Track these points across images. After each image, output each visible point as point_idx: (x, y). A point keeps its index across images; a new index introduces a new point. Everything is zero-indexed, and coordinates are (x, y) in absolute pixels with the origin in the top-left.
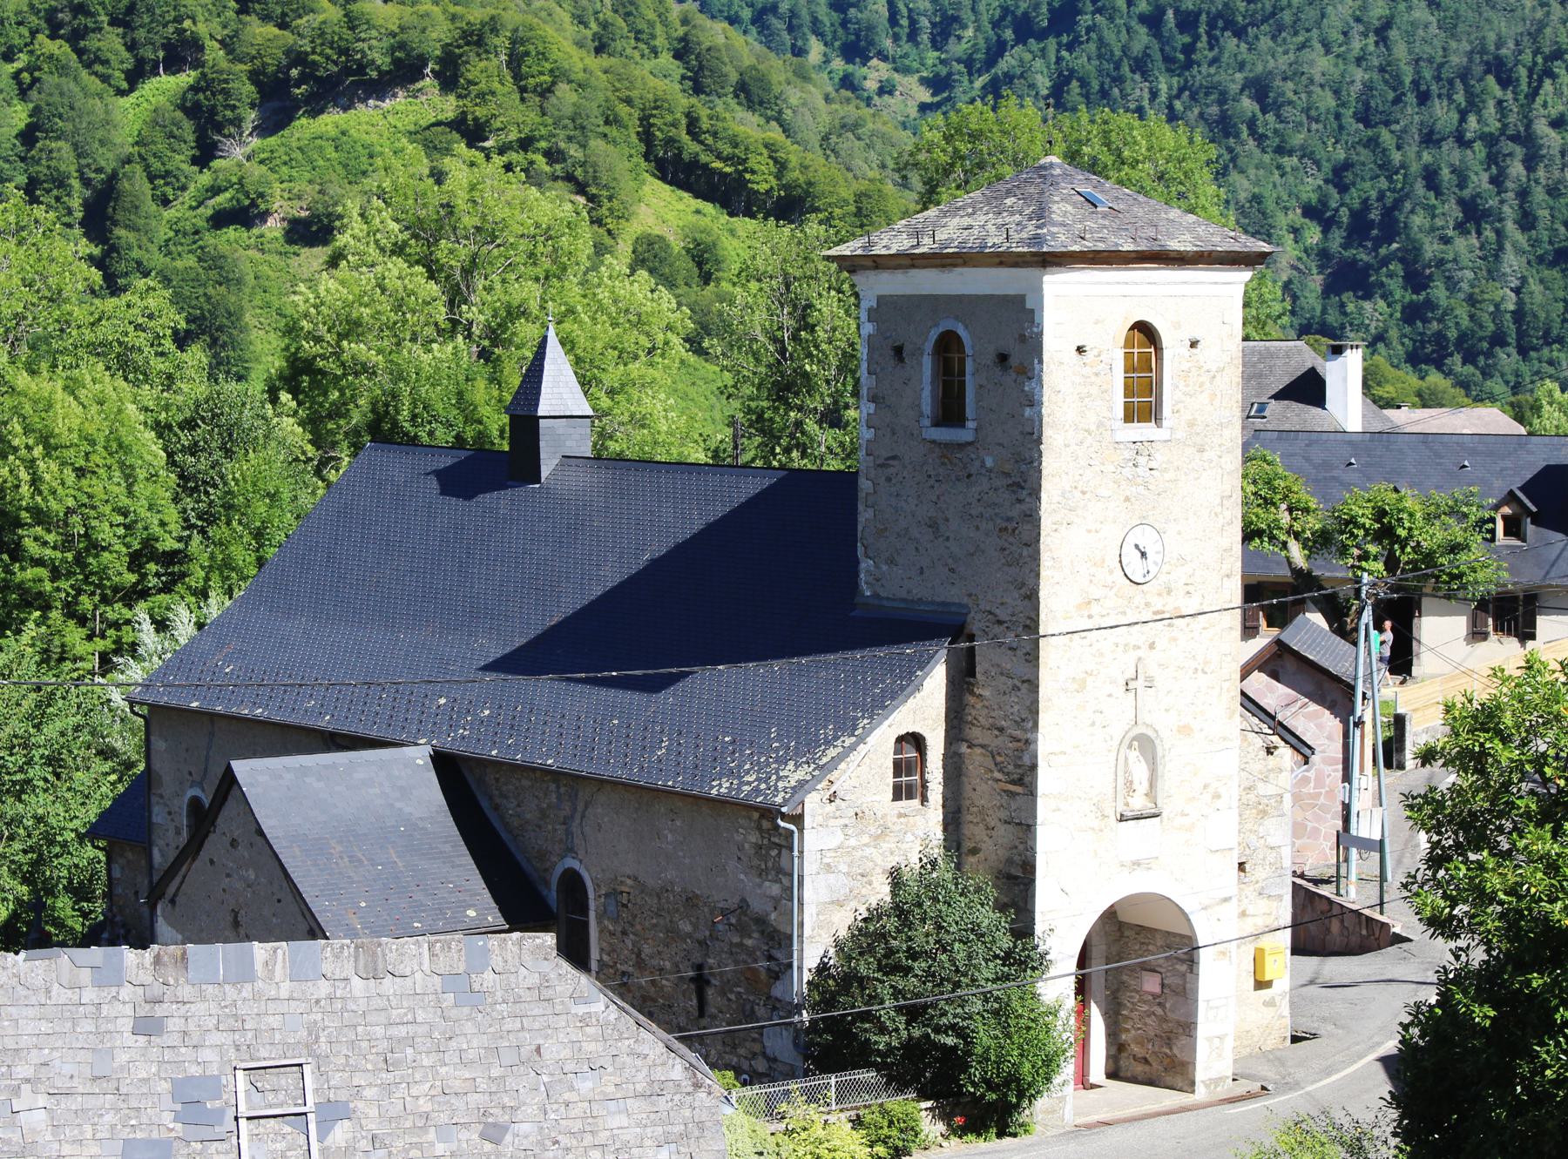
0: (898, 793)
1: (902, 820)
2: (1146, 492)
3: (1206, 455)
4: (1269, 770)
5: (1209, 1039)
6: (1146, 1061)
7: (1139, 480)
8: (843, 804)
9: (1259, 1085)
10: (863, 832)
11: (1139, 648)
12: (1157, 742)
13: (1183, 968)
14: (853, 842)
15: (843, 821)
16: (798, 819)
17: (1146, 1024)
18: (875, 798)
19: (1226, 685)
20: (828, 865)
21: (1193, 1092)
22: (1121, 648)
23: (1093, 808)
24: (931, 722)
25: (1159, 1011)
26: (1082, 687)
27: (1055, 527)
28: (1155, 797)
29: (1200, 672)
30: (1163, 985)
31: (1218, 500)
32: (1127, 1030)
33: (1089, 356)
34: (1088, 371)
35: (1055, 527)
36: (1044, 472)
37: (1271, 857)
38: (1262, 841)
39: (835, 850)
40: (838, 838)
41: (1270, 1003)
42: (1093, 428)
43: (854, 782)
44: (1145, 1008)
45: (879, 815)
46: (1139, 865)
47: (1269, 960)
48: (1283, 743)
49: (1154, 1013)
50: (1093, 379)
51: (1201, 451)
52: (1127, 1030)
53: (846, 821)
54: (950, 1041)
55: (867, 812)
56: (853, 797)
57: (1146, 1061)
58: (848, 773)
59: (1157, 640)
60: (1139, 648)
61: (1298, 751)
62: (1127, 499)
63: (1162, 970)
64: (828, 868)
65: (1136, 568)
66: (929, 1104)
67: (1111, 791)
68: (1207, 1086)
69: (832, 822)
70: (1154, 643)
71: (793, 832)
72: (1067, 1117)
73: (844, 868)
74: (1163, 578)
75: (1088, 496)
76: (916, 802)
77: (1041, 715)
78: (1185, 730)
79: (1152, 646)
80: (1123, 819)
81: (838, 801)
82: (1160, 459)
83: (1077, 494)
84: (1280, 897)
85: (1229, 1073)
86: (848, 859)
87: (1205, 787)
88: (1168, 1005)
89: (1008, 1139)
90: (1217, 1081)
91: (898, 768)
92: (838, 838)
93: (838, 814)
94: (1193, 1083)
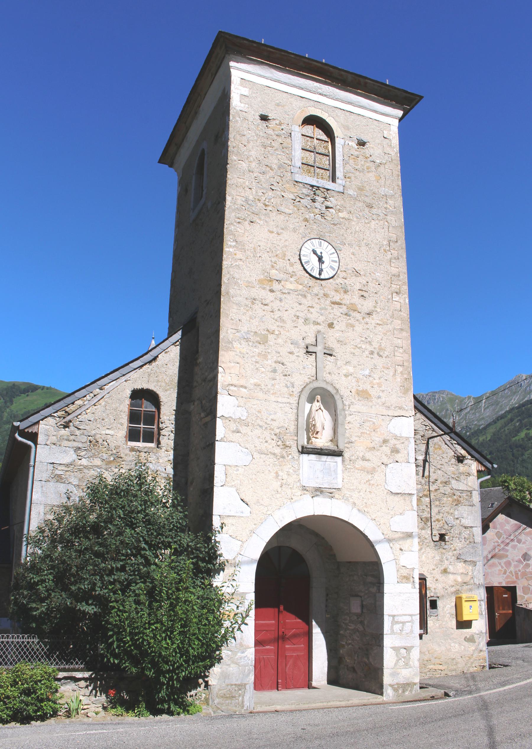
0: (133, 435)
1: (134, 453)
2: (323, 220)
3: (374, 211)
4: (460, 473)
5: (396, 649)
6: (354, 670)
7: (317, 211)
8: (78, 432)
9: (443, 691)
10: (94, 456)
11: (318, 324)
12: (337, 397)
13: (374, 590)
14: (84, 462)
15: (76, 444)
16: (34, 437)
17: (353, 640)
18: (108, 432)
19: (400, 369)
20: (59, 476)
21: (382, 694)
22: (301, 321)
23: (275, 437)
24: (163, 384)
25: (361, 628)
26: (264, 341)
27: (238, 220)
28: (337, 441)
29: (376, 355)
30: (362, 606)
31: (385, 243)
32: (343, 646)
33: (272, 124)
34: (270, 131)
35: (238, 220)
36: (229, 182)
37: (466, 533)
38: (458, 521)
39: (67, 465)
40: (70, 457)
41: (471, 640)
42: (274, 166)
43: (90, 416)
44: (352, 627)
45: (112, 446)
46: (322, 492)
47: (465, 606)
48: (469, 457)
49: (358, 631)
50: (275, 137)
51: (370, 206)
52: (343, 646)
53: (80, 445)
54: (90, 609)
55: (100, 441)
56: (87, 427)
57: (354, 670)
58: (83, 409)
59: (335, 322)
60: (318, 324)
61: (482, 464)
62: (306, 220)
63: (362, 594)
64: (59, 479)
65: (313, 264)
66: (87, 675)
67: (292, 428)
68: (395, 690)
69: (65, 443)
70: (332, 324)
71: (29, 447)
72: (247, 704)
73: (76, 482)
74: (339, 280)
75: (270, 208)
76: (152, 445)
77: (221, 353)
78: (364, 395)
79: (331, 325)
80: (304, 451)
81: (72, 428)
82: (332, 202)
83: (260, 205)
84: (474, 563)
85: (417, 680)
86: (80, 476)
87: (385, 441)
88: (366, 622)
89: (165, 717)
90: (406, 686)
91: (134, 417)
92: (70, 457)
93: (72, 438)
94: (381, 686)
